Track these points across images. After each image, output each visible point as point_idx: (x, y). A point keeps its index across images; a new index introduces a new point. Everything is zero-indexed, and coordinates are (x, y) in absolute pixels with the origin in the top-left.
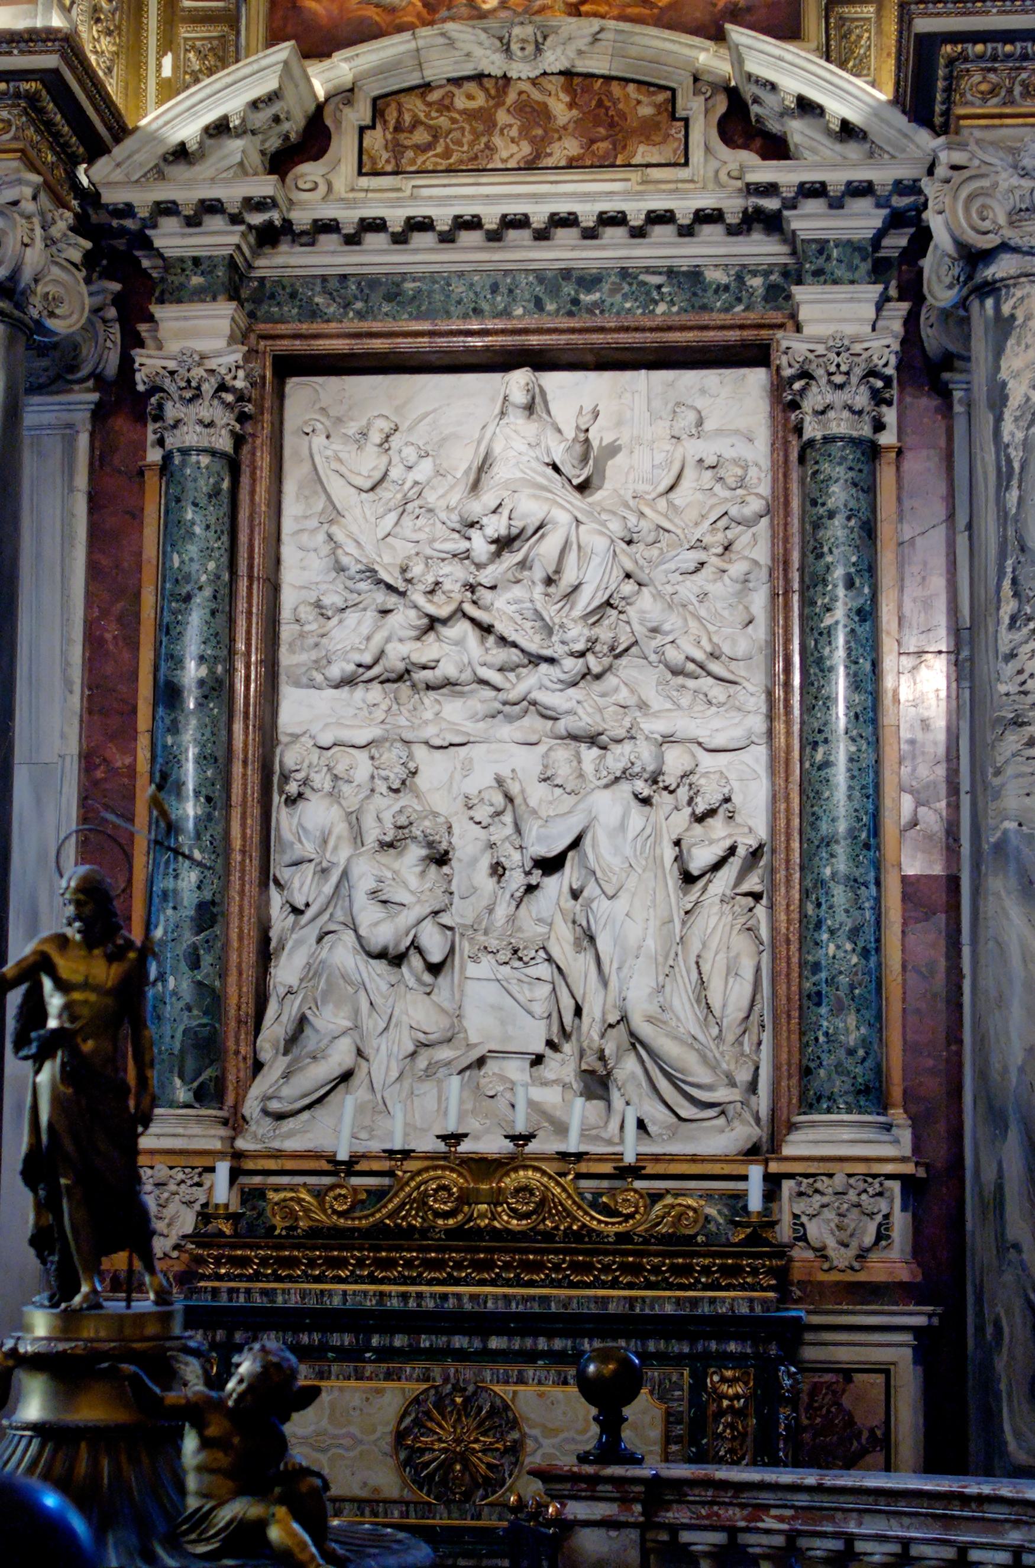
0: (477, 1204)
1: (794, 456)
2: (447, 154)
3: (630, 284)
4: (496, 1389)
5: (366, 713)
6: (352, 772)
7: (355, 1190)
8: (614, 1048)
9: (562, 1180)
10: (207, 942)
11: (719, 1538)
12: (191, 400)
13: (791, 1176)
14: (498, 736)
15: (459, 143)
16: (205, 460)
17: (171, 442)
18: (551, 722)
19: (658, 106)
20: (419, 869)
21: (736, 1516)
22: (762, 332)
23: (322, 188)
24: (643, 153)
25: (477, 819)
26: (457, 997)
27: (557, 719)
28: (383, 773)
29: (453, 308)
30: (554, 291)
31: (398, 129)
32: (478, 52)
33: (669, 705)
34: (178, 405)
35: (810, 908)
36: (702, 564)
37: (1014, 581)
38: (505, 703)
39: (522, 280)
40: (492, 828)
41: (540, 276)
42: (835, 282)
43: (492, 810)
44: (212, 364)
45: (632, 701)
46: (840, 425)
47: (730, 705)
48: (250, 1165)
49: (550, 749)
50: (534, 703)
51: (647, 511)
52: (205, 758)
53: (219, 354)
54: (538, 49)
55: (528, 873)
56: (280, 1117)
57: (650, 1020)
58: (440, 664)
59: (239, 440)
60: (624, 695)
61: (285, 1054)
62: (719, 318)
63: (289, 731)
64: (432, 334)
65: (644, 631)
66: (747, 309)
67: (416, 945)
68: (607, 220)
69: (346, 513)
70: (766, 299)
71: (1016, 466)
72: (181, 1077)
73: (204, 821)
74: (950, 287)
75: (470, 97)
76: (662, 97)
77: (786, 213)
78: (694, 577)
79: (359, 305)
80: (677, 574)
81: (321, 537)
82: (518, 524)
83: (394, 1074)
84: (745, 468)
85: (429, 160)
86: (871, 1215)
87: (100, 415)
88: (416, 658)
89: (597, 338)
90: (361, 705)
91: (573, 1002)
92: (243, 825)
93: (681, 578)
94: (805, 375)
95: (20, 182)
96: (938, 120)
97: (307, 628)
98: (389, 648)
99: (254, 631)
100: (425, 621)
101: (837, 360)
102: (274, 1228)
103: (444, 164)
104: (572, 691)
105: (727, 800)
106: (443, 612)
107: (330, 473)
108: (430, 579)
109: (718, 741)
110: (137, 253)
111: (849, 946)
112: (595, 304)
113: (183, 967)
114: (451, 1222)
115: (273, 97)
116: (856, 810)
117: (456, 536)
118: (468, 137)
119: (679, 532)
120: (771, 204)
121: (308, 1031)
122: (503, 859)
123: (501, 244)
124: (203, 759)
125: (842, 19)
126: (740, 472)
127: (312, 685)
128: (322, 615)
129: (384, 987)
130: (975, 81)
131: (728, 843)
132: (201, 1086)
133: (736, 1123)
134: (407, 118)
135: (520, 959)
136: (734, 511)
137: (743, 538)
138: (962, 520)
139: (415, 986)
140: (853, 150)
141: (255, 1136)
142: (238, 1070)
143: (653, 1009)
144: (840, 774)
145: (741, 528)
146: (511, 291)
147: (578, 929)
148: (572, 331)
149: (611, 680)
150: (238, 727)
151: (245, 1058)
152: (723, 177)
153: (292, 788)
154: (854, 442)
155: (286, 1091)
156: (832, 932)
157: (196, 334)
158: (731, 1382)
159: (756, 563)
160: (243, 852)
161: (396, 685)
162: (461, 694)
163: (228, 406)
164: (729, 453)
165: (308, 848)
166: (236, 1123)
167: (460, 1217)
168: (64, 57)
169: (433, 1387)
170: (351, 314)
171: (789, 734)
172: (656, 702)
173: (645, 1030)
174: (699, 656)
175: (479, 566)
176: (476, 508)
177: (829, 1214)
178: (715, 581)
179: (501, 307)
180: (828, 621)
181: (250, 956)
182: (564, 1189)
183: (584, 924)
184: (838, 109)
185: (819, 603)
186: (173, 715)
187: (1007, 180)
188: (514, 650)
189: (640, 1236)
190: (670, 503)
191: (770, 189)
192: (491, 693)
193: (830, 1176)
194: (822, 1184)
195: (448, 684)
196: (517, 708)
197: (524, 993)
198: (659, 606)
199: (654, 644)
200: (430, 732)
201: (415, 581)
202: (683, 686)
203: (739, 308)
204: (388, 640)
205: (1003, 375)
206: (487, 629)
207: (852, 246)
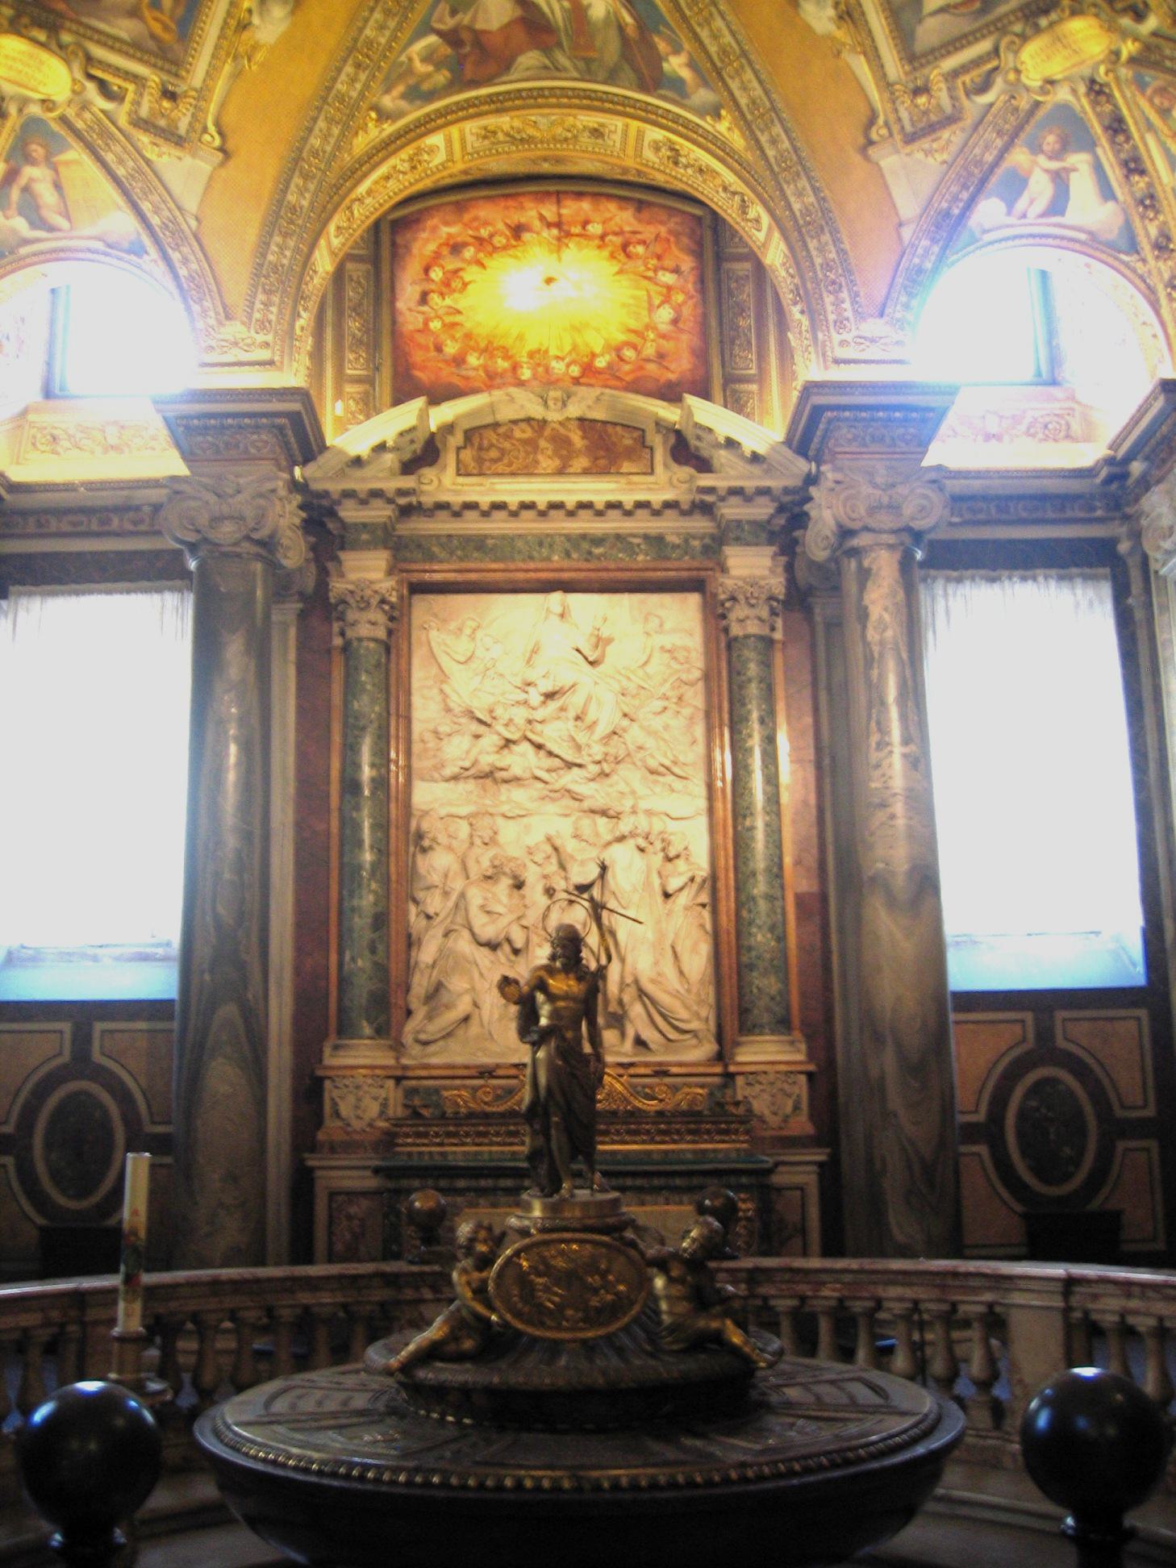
1: (723, 645)
2: (510, 464)
7: (494, 1088)
11: (794, 1302)
12: (362, 609)
15: (517, 458)
16: (372, 645)
17: (350, 633)
19: (635, 440)
21: (805, 1289)
23: (436, 482)
24: (626, 467)
30: (577, 547)
31: (481, 448)
32: (528, 405)
35: (745, 914)
37: (878, 723)
39: (557, 539)
41: (568, 537)
42: (748, 544)
44: (377, 587)
45: (626, 790)
46: (753, 628)
48: (410, 1074)
50: (568, 791)
53: (380, 581)
54: (564, 404)
56: (426, 1043)
57: (653, 981)
59: (390, 632)
60: (622, 787)
62: (676, 564)
67: (509, 940)
68: (611, 506)
71: (876, 655)
72: (368, 1020)
73: (375, 866)
74: (825, 549)
75: (523, 431)
76: (636, 434)
79: (459, 553)
81: (435, 691)
83: (496, 1016)
85: (500, 467)
86: (789, 1096)
87: (303, 616)
89: (604, 575)
94: (733, 599)
95: (277, 478)
96: (811, 453)
100: (502, 742)
103: (508, 470)
104: (592, 784)
105: (686, 849)
108: (506, 717)
112: (602, 555)
113: (367, 953)
115: (412, 429)
118: (522, 454)
121: (443, 991)
124: (373, 827)
125: (734, 392)
127: (433, 780)
130: (844, 432)
131: (690, 874)
134: (486, 443)
136: (684, 677)
138: (822, 684)
140: (756, 470)
143: (653, 975)
144: (760, 835)
146: (551, 546)
148: (589, 570)
149: (614, 778)
150: (393, 806)
152: (675, 482)
153: (426, 843)
154: (762, 638)
156: (759, 927)
158: (744, 1201)
165: (436, 878)
166: (398, 1047)
168: (303, 404)
171: (725, 809)
172: (641, 790)
173: (649, 988)
174: (667, 763)
176: (532, 676)
177: (766, 1096)
180: (750, 743)
181: (402, 946)
184: (749, 445)
187: (866, 489)
191: (711, 490)
192: (541, 785)
193: (765, 1073)
194: (761, 1078)
195: (517, 780)
200: (505, 809)
204: (480, 753)
205: (867, 601)
206: (539, 747)
207: (754, 523)
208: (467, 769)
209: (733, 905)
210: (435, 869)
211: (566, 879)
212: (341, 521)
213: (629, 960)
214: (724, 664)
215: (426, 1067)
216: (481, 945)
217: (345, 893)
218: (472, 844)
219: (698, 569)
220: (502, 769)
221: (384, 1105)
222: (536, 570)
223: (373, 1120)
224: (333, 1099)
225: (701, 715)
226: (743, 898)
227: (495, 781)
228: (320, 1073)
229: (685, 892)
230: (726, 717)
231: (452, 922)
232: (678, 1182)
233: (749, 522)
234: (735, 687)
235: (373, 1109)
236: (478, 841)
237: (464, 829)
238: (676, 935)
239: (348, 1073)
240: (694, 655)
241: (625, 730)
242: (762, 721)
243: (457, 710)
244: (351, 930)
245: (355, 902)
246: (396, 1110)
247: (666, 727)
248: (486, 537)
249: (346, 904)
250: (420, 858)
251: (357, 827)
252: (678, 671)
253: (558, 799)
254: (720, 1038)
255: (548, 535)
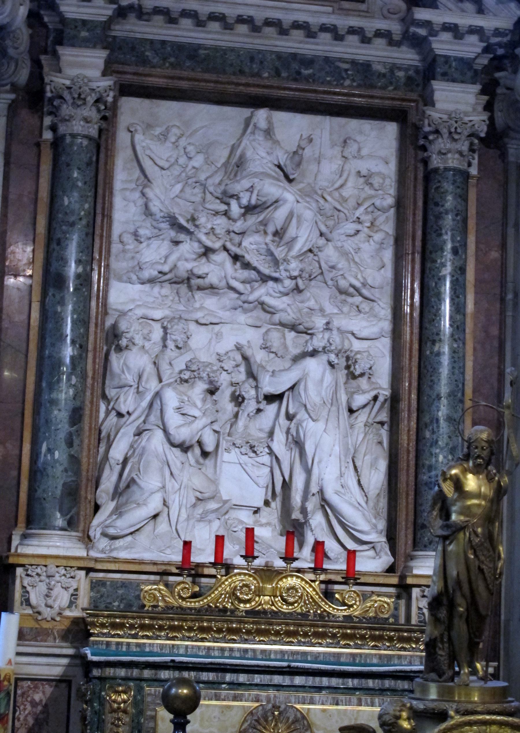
0: (264, 596)
1: (420, 175)
3: (330, 67)
4: (298, 706)
5: (160, 300)
6: (150, 335)
8: (313, 507)
9: (313, 584)
10: (77, 431)
13: (419, 586)
14: (238, 321)
16: (85, 142)
17: (62, 129)
18: (269, 316)
20: (202, 396)
22: (404, 103)
25: (226, 368)
26: (218, 472)
27: (275, 314)
28: (173, 337)
29: (227, 68)
33: (336, 311)
34: (70, 108)
35: (428, 434)
36: (358, 231)
38: (244, 302)
40: (233, 374)
41: (279, 56)
42: (454, 81)
43: (234, 363)
44: (94, 85)
45: (317, 307)
47: (373, 315)
48: (99, 566)
49: (268, 330)
51: (328, 198)
52: (80, 321)
55: (258, 402)
56: (114, 538)
58: (209, 276)
60: (312, 303)
61: (113, 500)
63: (114, 307)
64: (216, 82)
65: (327, 267)
66: (395, 89)
69: (153, 181)
70: (405, 84)
72: (60, 511)
77: (431, 38)
78: (351, 238)
80: (343, 236)
81: (137, 194)
82: (264, 199)
83: (184, 515)
84: (384, 179)
88: (197, 271)
90: (157, 295)
91: (282, 478)
92: (94, 362)
93: (346, 238)
94: (437, 132)
97: (128, 247)
98: (179, 264)
99: (104, 247)
100: (203, 250)
101: (456, 125)
102: (144, 606)
104: (285, 298)
105: (370, 368)
106: (217, 245)
107: (144, 156)
108: (209, 226)
109: (364, 334)
110: (42, 12)
111: (450, 457)
113: (63, 445)
114: (248, 605)
116: (456, 381)
117: (218, 201)
119: (346, 211)
120: (422, 32)
121: (134, 488)
122: (243, 393)
123: (260, 34)
126: (381, 181)
128: (137, 240)
129: (179, 464)
132: (71, 517)
133: (382, 554)
135: (255, 452)
136: (378, 203)
137: (382, 219)
139: (195, 465)
141: (98, 549)
142: (86, 509)
145: (379, 213)
146: (262, 62)
147: (290, 437)
149: (307, 294)
150: (93, 303)
151: (90, 502)
153: (124, 342)
154: (457, 171)
155: (120, 523)
156: (442, 449)
157: (83, 66)
159: (387, 233)
160: (93, 378)
161: (179, 286)
162: (217, 294)
163: (99, 111)
164: (374, 169)
165: (129, 378)
167: (253, 603)
169: (261, 705)
170: (167, 65)
171: (412, 333)
172: (330, 309)
174: (358, 284)
175: (235, 221)
178: (364, 242)
179: (256, 70)
182: (314, 590)
183: (295, 434)
185: (439, 261)
186: (62, 295)
188: (253, 272)
189: (357, 617)
190: (341, 195)
191: (427, 24)
195: (212, 287)
196: (251, 305)
197: (256, 472)
198: (337, 254)
199: (331, 275)
200: (199, 315)
201: (200, 226)
202: (345, 301)
203: (391, 88)
204: (179, 259)
208: (165, 274)
209: (413, 424)
210: (128, 368)
211: (257, 387)
212: (60, 14)
213: (315, 471)
214: (420, 195)
215: (116, 560)
216: (173, 445)
217: (44, 384)
218: (165, 346)
219: (403, 100)
220: (199, 277)
221: (75, 595)
222: (247, 85)
223: (61, 609)
224: (24, 587)
225: (391, 241)
226: (426, 419)
227: (190, 287)
228: (12, 560)
229: (367, 410)
230: (418, 244)
231: (144, 422)
232: (370, 683)
233: (456, 59)
234: (431, 217)
235: (64, 599)
236: (171, 344)
237: (157, 333)
238: (356, 451)
239: (42, 562)
240: (388, 182)
241: (320, 249)
242: (455, 251)
243: (159, 215)
244: (47, 422)
245: (54, 395)
246: (84, 601)
247: (358, 250)
248: (200, 46)
249: (46, 397)
250: (114, 357)
251: (59, 321)
252: (371, 197)
253: (251, 311)
254: (393, 551)
255: (259, 52)
